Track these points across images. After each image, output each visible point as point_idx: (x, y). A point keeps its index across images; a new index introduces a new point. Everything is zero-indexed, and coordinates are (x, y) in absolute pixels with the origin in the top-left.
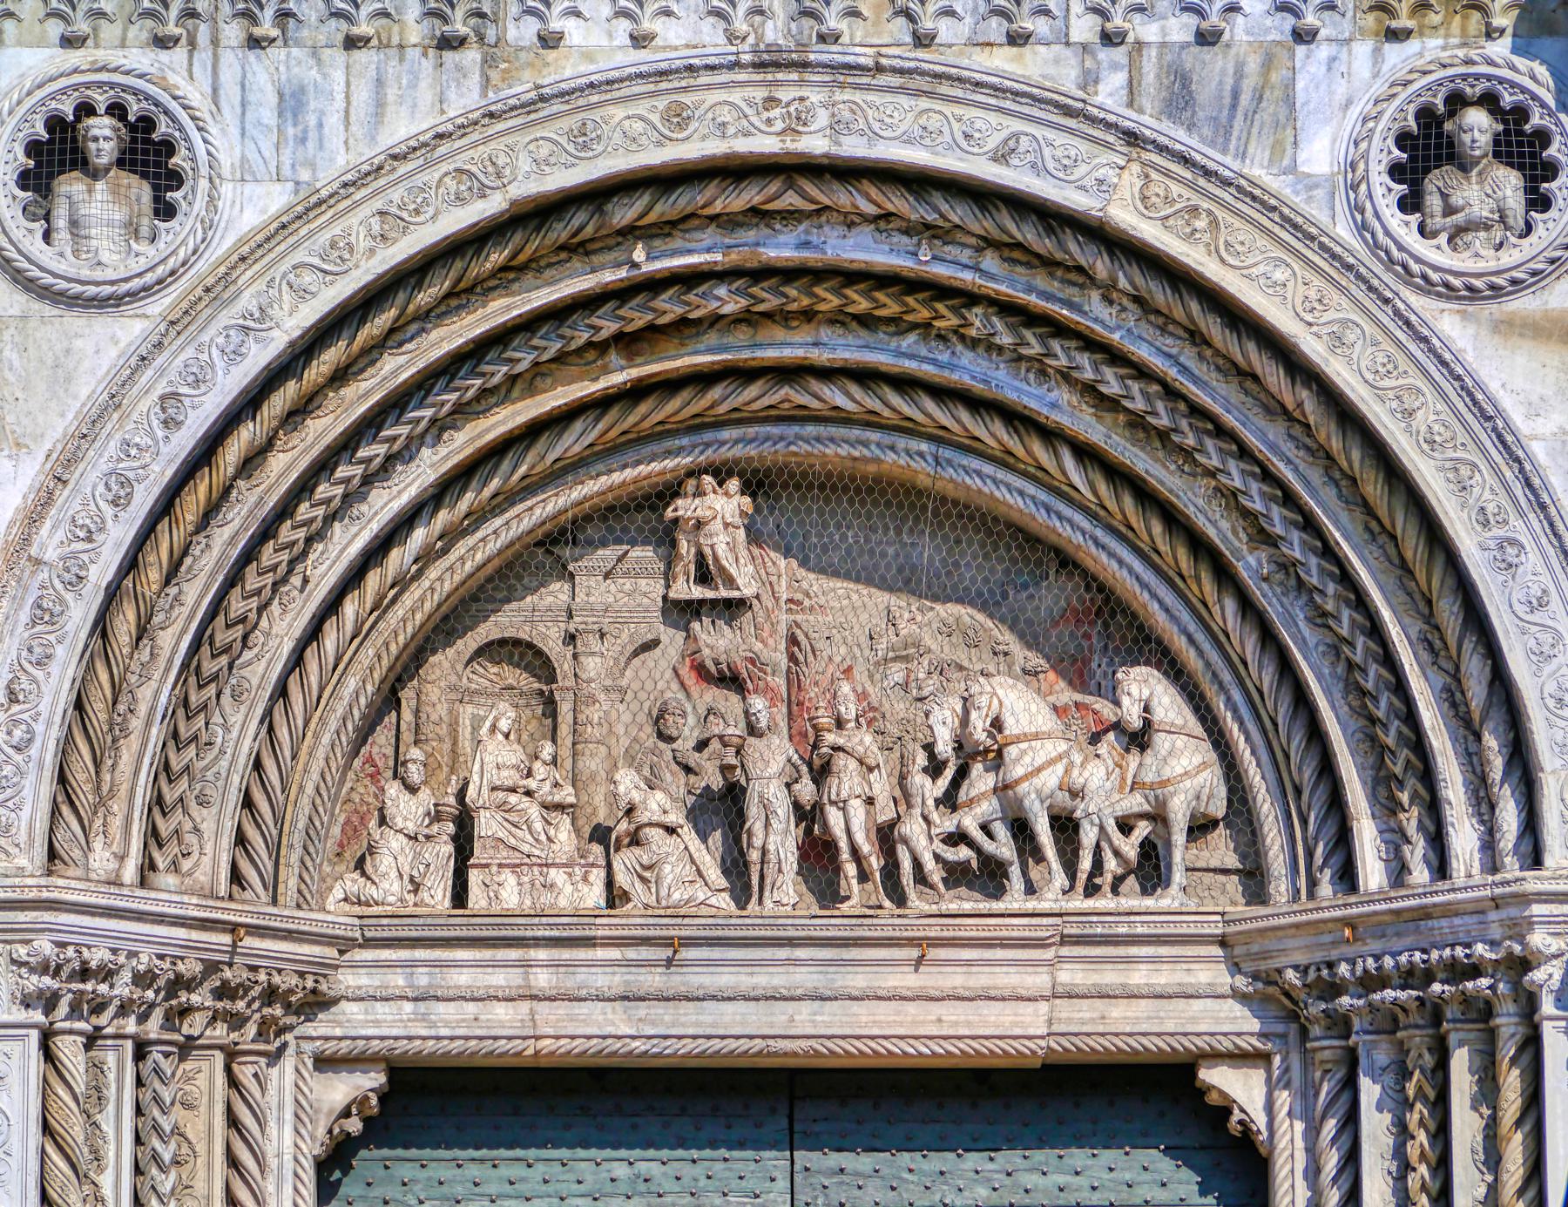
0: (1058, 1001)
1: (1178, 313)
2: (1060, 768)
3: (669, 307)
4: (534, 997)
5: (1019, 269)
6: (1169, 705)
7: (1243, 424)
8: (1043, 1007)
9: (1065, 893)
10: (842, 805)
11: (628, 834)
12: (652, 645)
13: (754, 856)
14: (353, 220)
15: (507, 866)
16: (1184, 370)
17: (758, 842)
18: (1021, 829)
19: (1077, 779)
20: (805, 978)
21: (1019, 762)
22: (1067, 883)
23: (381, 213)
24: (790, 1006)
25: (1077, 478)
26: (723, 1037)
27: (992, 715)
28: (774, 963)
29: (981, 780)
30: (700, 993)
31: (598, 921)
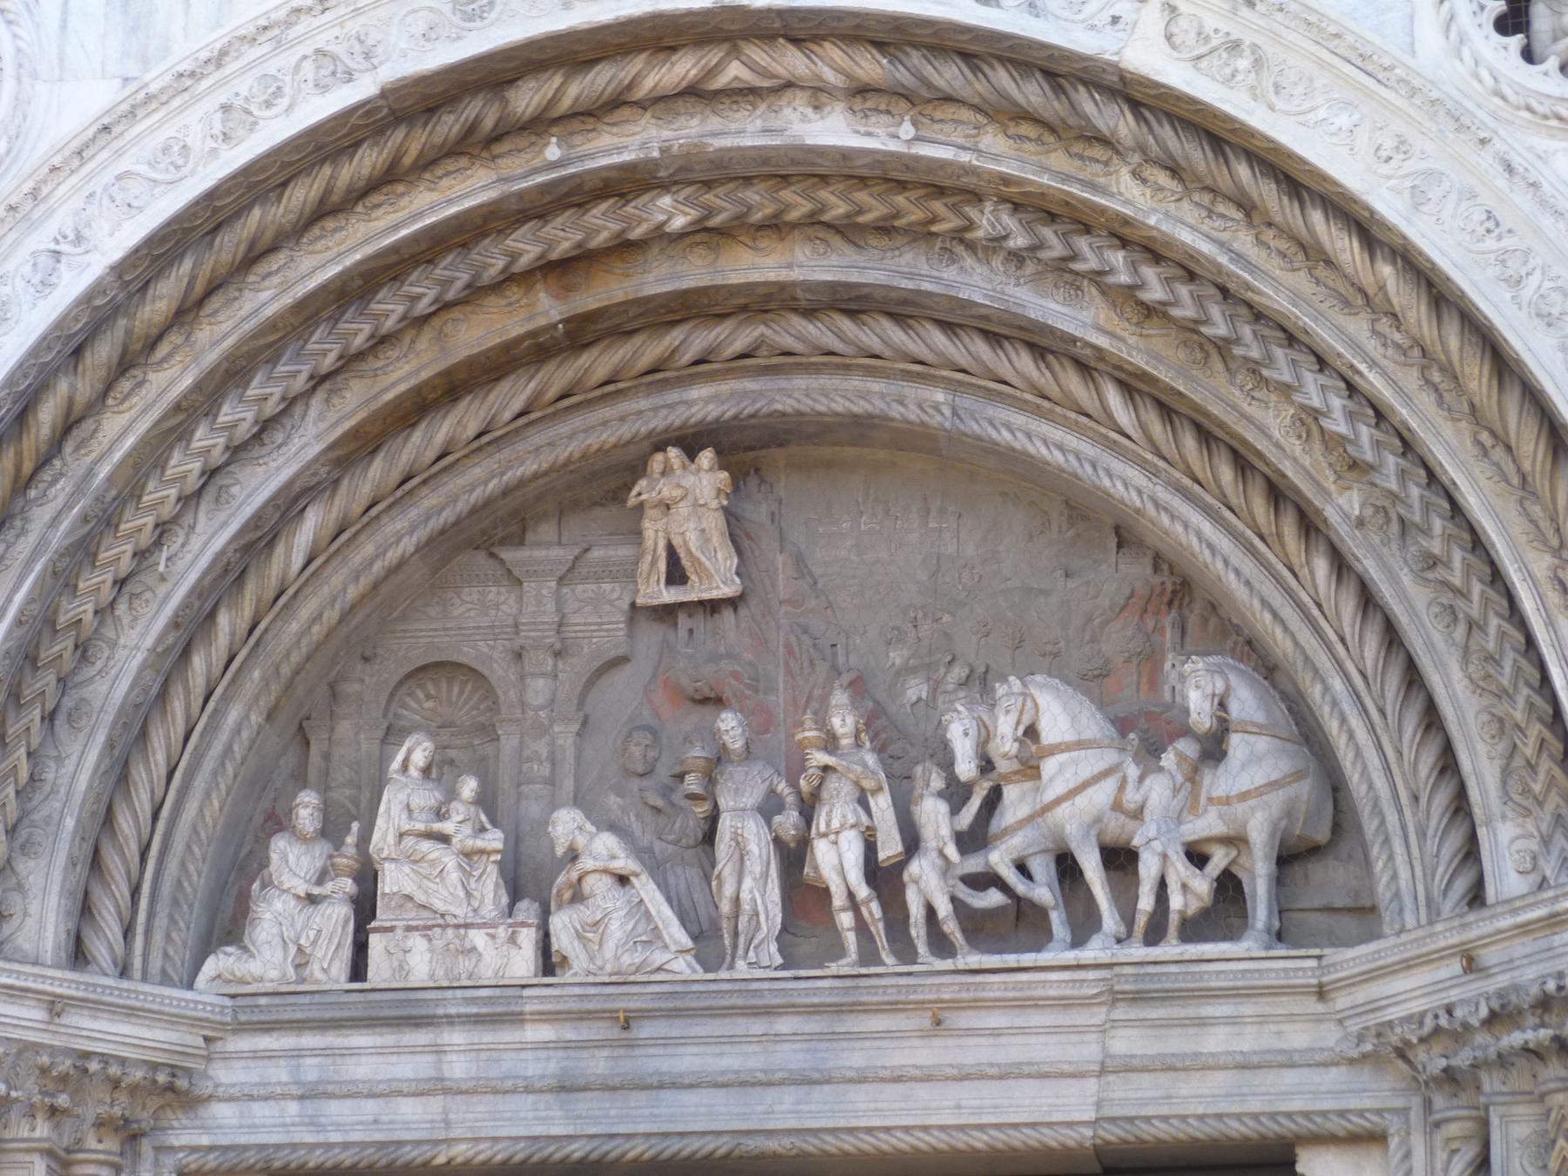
0: (1111, 1078)
1: (1224, 181)
2: (1108, 787)
3: (602, 223)
4: (447, 1091)
5: (1028, 146)
6: (1246, 703)
7: (1315, 320)
8: (1091, 1085)
9: (1119, 941)
10: (832, 835)
11: (570, 886)
12: (620, 661)
13: (725, 907)
14: (193, 117)
15: (416, 928)
16: (1239, 257)
17: (729, 890)
18: (1067, 867)
19: (1132, 797)
20: (790, 1057)
21: (1058, 773)
22: (1123, 929)
23: (226, 108)
24: (771, 1094)
25: (1123, 416)
26: (682, 1135)
27: (1026, 721)
28: (747, 1039)
29: (1016, 803)
30: (655, 1080)
31: (527, 992)
